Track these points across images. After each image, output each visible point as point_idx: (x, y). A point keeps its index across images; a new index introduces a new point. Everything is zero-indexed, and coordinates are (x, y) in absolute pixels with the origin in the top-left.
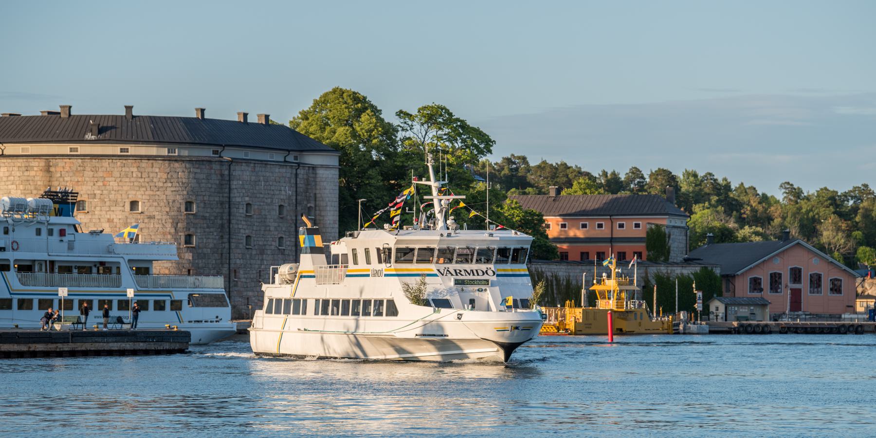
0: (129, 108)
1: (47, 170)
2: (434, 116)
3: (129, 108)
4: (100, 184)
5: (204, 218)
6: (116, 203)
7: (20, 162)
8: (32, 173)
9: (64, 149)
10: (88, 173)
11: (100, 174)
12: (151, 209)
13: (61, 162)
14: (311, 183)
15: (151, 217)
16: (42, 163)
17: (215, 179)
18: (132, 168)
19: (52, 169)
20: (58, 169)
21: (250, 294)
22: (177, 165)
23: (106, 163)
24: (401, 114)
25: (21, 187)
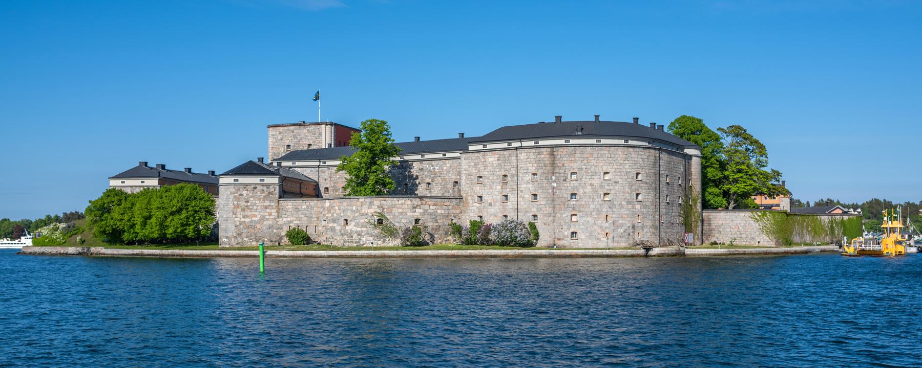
0: (597, 117)
1: (552, 154)
2: (738, 132)
3: (597, 117)
5: (646, 183)
6: (595, 173)
7: (533, 150)
8: (542, 156)
9: (562, 142)
10: (578, 155)
14: (690, 165)
15: (616, 182)
16: (549, 150)
17: (652, 158)
18: (605, 151)
22: (631, 149)
23: (589, 149)
24: (720, 129)
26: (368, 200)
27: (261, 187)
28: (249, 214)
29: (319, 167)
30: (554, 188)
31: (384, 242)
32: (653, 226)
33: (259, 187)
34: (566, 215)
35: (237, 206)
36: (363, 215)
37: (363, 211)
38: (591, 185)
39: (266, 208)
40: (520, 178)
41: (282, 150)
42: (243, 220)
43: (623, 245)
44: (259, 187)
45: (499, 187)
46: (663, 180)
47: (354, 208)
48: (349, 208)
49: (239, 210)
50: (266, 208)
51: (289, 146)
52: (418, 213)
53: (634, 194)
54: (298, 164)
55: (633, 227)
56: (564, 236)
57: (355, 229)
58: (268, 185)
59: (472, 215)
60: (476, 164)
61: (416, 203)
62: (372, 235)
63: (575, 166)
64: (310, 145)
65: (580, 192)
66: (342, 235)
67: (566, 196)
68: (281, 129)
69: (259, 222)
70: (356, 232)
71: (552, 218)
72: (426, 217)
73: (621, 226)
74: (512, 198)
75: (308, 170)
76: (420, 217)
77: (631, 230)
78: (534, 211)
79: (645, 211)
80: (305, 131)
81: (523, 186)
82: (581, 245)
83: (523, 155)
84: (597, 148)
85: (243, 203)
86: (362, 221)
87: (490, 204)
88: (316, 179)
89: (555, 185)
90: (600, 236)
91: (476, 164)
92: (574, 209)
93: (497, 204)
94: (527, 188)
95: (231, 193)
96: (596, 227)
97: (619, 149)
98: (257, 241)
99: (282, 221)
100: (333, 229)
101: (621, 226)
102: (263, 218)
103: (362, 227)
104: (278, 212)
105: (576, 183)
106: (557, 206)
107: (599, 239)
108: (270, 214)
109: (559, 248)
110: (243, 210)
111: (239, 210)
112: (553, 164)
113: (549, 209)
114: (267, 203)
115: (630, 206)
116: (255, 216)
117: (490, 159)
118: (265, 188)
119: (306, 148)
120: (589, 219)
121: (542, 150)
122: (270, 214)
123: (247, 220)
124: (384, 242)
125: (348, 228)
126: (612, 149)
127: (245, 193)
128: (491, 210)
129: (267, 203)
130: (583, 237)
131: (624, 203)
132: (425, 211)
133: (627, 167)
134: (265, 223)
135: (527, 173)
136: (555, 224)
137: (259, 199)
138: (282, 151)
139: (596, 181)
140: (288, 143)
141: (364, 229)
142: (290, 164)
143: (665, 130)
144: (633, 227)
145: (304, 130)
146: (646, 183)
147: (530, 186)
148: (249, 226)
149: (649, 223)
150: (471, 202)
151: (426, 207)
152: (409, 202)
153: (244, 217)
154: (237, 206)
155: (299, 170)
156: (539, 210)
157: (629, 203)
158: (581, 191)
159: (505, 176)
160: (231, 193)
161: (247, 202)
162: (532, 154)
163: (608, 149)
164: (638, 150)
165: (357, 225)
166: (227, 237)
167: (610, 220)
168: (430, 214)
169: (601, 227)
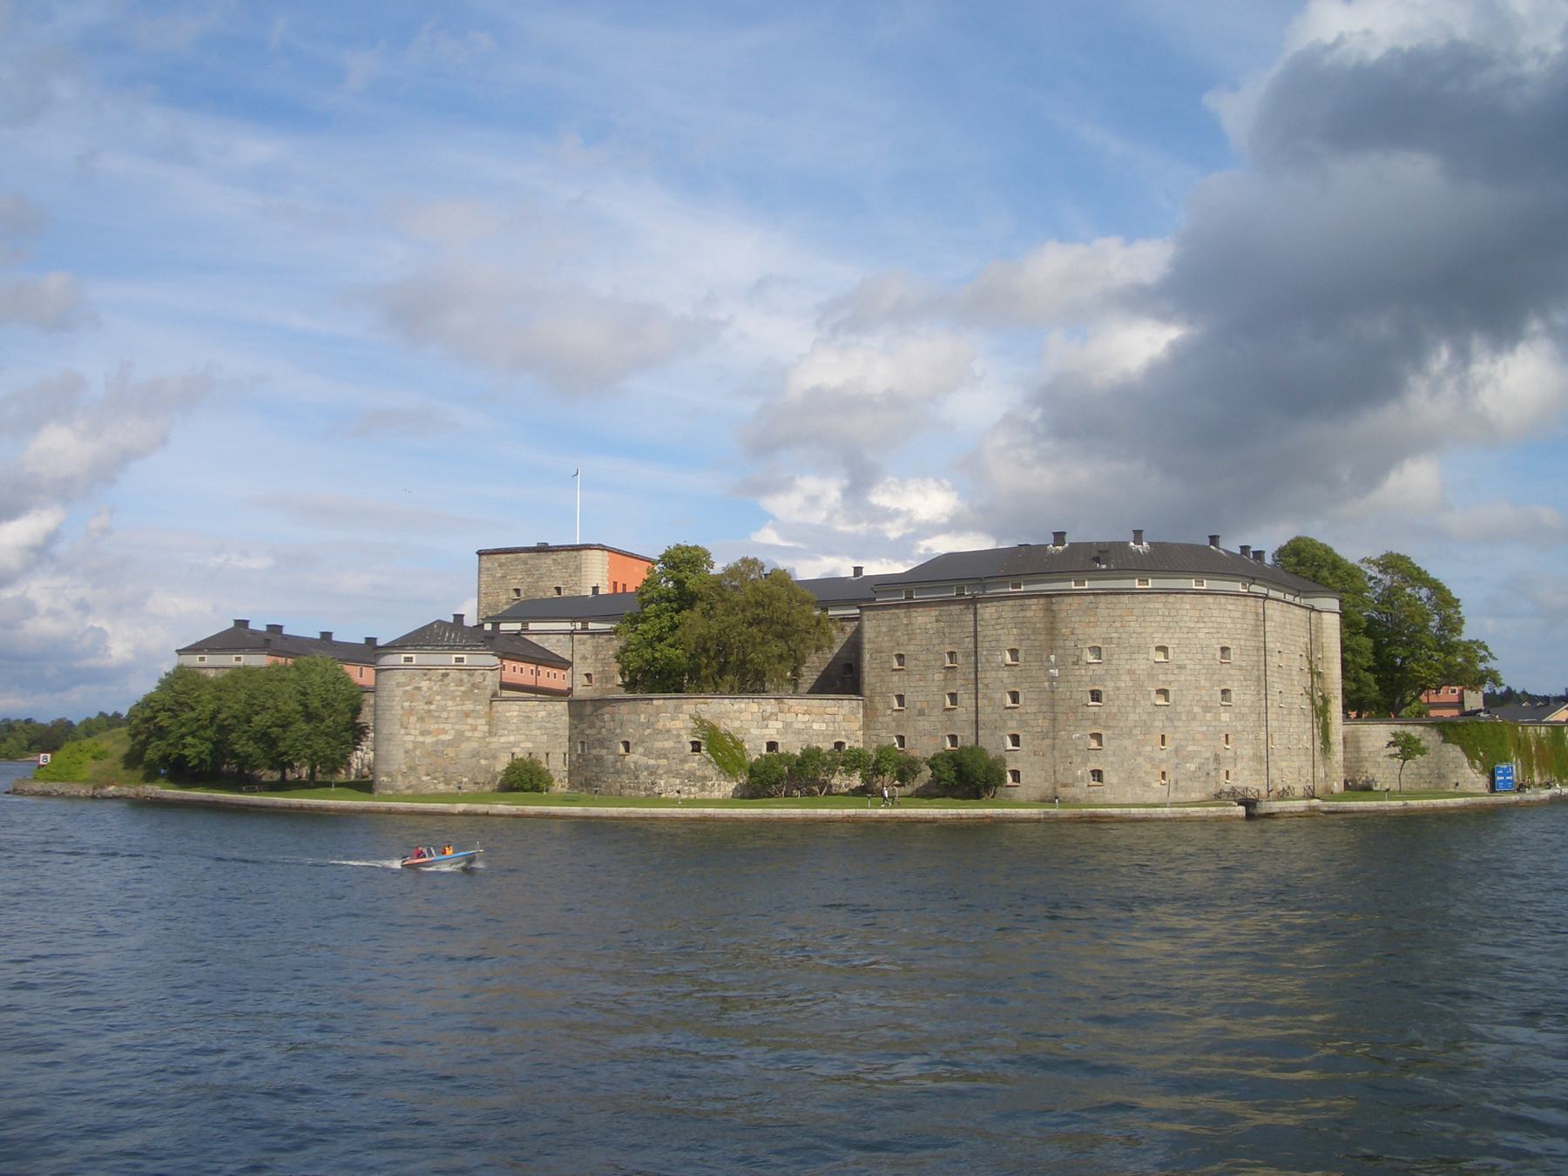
1: (1049, 610)
4: (1118, 624)
5: (1241, 668)
6: (1138, 649)
8: (1029, 614)
11: (1118, 613)
12: (1183, 656)
13: (1069, 600)
14: (1319, 629)
16: (1042, 601)
18: (1158, 603)
19: (1055, 607)
20: (1063, 607)
21: (1284, 764)
22: (1210, 599)
25: (1015, 631)
26: (671, 703)
27: (458, 674)
28: (434, 727)
29: (572, 633)
30: (1053, 679)
31: (702, 790)
32: (1257, 758)
33: (453, 674)
34: (1080, 735)
35: (411, 711)
36: (660, 732)
37: (660, 726)
38: (1131, 672)
39: (467, 715)
40: (982, 659)
41: (503, 598)
42: (420, 739)
43: (1196, 796)
44: (453, 674)
45: (939, 677)
46: (1274, 660)
47: (643, 718)
48: (633, 718)
49: (413, 719)
50: (467, 715)
51: (517, 591)
52: (772, 731)
53: (1218, 690)
54: (532, 626)
55: (1217, 758)
56: (1076, 779)
57: (644, 760)
58: (470, 671)
59: (883, 733)
60: (892, 630)
61: (769, 709)
62: (677, 775)
63: (1096, 634)
64: (558, 589)
65: (1107, 688)
66: (618, 772)
67: (1077, 696)
68: (503, 557)
69: (450, 744)
70: (647, 767)
71: (1048, 742)
72: (790, 737)
73: (1190, 757)
74: (966, 700)
75: (554, 638)
76: (776, 738)
77: (1212, 766)
78: (1013, 726)
79: (1239, 725)
80: (549, 561)
81: (988, 676)
82: (1109, 798)
83: (988, 612)
84: (1141, 597)
85: (420, 706)
86: (658, 745)
87: (921, 713)
88: (567, 657)
89: (1055, 672)
90: (1149, 779)
91: (892, 630)
92: (1095, 722)
93: (937, 712)
94: (998, 680)
95: (399, 685)
96: (1140, 759)
97: (1187, 598)
98: (447, 783)
99: (496, 742)
100: (599, 759)
101: (1190, 757)
102: (460, 734)
103: (659, 757)
104: (489, 724)
105: (1099, 670)
106: (1061, 717)
107: (1146, 785)
108: (474, 728)
109: (1065, 803)
110: (421, 719)
111: (413, 719)
112: (1052, 631)
113: (1043, 723)
114: (469, 706)
115: (1209, 716)
116: (445, 732)
117: (920, 620)
118: (465, 676)
119: (553, 594)
120: (1126, 743)
121: (1027, 602)
122: (474, 728)
123: (429, 740)
124: (702, 790)
125: (631, 758)
126: (1171, 598)
127: (425, 685)
128: (923, 724)
129: (469, 706)
130: (1114, 780)
131: (1196, 709)
132: (787, 725)
133: (1201, 635)
134: (463, 746)
135: (998, 648)
136: (1056, 753)
137: (453, 698)
138: (504, 600)
139: (1140, 665)
140: (515, 584)
141: (664, 762)
142: (517, 626)
143: (1268, 560)
144: (1217, 758)
145: (548, 560)
146: (1241, 668)
147: (1005, 674)
148: (436, 752)
149: (1247, 751)
150: (880, 706)
151: (790, 717)
152: (754, 707)
153: (423, 733)
154: (411, 711)
155: (534, 639)
156: (1023, 723)
157: (1207, 709)
158: (1110, 684)
159: (951, 654)
160: (399, 685)
161: (430, 703)
162: (1007, 609)
163: (1163, 598)
164: (1222, 599)
165: (647, 753)
166: (388, 774)
167: (1169, 746)
168: (798, 732)
169: (1152, 759)
